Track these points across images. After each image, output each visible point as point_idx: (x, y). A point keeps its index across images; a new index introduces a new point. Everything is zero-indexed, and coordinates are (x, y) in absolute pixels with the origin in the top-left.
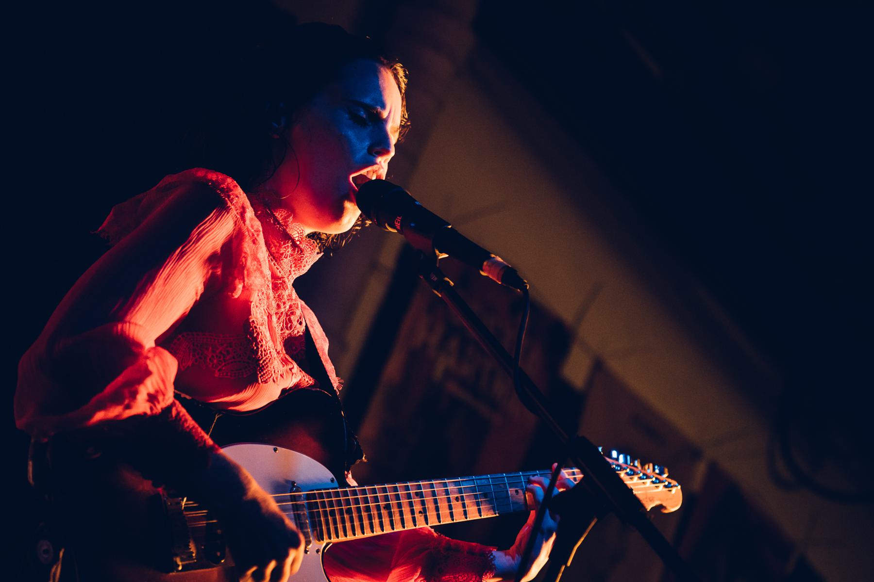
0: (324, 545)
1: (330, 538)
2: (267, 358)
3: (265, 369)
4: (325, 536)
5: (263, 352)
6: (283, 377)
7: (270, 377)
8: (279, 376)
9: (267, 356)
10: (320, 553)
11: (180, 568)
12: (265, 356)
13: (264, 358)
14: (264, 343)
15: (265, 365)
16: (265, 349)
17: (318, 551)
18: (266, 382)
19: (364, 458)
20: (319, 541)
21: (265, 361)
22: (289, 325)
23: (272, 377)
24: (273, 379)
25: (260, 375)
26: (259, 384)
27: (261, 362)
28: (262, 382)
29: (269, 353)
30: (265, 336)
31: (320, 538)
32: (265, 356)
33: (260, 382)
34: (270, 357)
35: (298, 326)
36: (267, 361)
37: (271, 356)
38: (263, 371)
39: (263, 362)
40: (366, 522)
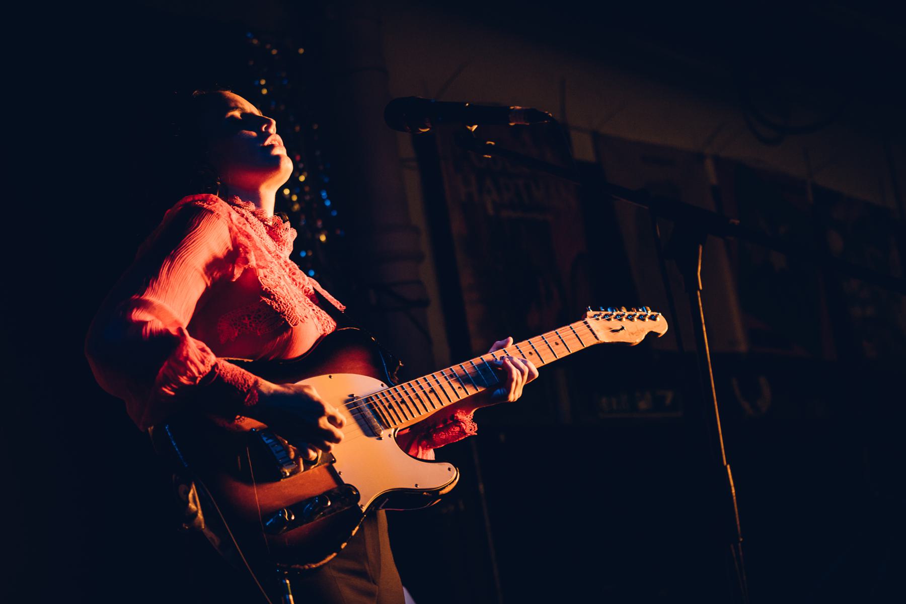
0: (393, 430)
1: (395, 424)
2: (289, 309)
4: (392, 424)
5: (284, 306)
9: (288, 307)
10: (392, 436)
11: (288, 474)
12: (287, 307)
13: (287, 309)
17: (390, 436)
18: (295, 325)
19: (401, 364)
20: (388, 428)
21: (288, 311)
24: (301, 321)
25: (289, 321)
26: (292, 327)
27: (286, 312)
28: (293, 325)
29: (289, 304)
31: (387, 427)
32: (287, 307)
33: (292, 326)
34: (291, 307)
36: (290, 310)
38: (290, 318)
40: (420, 407)
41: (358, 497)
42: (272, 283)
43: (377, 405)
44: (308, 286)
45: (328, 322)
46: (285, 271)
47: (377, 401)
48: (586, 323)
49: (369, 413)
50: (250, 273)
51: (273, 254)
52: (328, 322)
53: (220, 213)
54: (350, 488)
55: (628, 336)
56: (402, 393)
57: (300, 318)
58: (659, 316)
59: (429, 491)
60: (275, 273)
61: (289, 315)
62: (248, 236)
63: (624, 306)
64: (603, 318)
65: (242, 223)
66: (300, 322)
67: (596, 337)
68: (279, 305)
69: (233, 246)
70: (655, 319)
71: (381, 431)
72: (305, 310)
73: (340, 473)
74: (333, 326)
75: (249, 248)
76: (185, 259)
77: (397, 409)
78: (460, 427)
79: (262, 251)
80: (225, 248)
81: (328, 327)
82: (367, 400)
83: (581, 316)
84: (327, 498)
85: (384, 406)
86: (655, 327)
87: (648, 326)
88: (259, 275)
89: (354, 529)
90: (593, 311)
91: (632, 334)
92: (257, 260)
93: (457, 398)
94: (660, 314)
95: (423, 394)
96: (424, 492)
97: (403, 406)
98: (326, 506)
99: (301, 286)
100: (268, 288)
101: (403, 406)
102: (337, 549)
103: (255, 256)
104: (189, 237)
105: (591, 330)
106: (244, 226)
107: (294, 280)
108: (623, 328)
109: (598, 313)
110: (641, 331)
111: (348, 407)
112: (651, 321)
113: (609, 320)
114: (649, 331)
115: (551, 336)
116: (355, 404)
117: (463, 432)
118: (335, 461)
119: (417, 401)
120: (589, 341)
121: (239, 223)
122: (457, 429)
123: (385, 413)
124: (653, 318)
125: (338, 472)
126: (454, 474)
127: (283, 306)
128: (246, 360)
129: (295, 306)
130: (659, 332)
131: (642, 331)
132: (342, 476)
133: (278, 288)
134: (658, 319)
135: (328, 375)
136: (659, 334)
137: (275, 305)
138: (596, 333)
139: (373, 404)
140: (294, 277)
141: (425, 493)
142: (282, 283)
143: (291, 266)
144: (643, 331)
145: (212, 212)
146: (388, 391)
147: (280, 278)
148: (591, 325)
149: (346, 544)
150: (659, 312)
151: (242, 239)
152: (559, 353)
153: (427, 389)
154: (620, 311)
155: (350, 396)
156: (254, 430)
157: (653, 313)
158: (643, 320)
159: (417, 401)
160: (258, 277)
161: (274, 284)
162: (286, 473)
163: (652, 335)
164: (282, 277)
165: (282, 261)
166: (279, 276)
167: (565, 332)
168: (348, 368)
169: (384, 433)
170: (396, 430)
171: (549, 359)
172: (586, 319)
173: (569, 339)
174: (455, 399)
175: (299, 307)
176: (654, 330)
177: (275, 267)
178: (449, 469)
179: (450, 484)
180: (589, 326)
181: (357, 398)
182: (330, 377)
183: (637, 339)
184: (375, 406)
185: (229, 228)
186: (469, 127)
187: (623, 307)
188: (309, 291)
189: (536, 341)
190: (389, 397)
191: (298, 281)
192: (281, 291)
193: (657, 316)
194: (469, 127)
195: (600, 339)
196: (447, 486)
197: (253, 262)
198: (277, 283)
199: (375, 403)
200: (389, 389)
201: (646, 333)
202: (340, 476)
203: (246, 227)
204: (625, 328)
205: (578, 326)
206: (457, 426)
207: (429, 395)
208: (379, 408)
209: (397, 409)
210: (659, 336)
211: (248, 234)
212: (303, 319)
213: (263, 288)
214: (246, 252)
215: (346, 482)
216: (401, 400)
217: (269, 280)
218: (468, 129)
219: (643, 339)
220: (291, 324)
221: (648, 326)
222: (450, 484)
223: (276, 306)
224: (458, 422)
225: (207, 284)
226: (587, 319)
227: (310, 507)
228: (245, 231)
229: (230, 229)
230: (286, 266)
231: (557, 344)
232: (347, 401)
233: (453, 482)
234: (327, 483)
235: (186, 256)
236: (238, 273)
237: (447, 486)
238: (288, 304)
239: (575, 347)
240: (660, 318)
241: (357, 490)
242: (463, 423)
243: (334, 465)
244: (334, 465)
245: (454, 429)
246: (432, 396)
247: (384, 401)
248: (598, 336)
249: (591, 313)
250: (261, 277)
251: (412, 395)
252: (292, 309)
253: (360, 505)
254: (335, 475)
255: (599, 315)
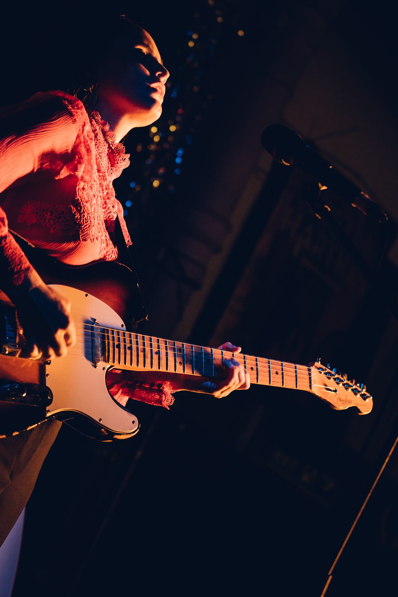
0: (109, 366)
1: (114, 362)
2: (87, 225)
3: (85, 232)
5: (85, 220)
6: (97, 239)
7: (89, 238)
8: (95, 238)
9: (88, 223)
10: (105, 370)
11: (7, 352)
12: (86, 223)
13: (85, 224)
14: (86, 214)
15: (86, 229)
16: (87, 218)
17: (104, 369)
18: (85, 240)
19: (147, 318)
20: (106, 362)
21: (84, 227)
22: (104, 206)
23: (90, 238)
24: (91, 239)
25: (81, 235)
26: (81, 241)
27: (83, 226)
28: (82, 240)
29: (89, 221)
30: (88, 209)
31: (106, 360)
32: (86, 223)
33: (81, 240)
34: (90, 224)
35: (111, 208)
36: (87, 226)
37: (91, 223)
38: (83, 233)
39: (84, 227)
40: (141, 359)
41: (50, 402)
42: (86, 197)
43: (108, 339)
44: (113, 214)
45: (113, 251)
46: (103, 193)
47: (110, 335)
48: (309, 370)
49: (98, 341)
50: (73, 180)
51: (101, 174)
52: (113, 251)
53: (78, 120)
54: (48, 392)
55: (336, 400)
56: (134, 340)
57: (91, 237)
58: (369, 398)
59: (107, 430)
60: (93, 191)
61: (84, 230)
62: (88, 150)
63: (347, 375)
64: (326, 374)
65: (90, 137)
66: (89, 240)
67: (310, 386)
68: (81, 217)
69: (72, 151)
70: (365, 399)
71: (99, 361)
72: (99, 232)
73: (48, 375)
74: (114, 257)
75: (84, 160)
76: (29, 141)
77: (122, 351)
78: (161, 397)
79: (92, 168)
80: (65, 149)
81: (110, 256)
82: (103, 331)
83: (309, 363)
84: (26, 389)
85: (114, 344)
86: (361, 405)
87: (356, 401)
88: (78, 185)
89: (31, 426)
90: (321, 364)
91: (340, 400)
92: (84, 172)
93: (174, 370)
94: (371, 398)
95: (149, 352)
96: (103, 428)
97: (128, 352)
98: (20, 395)
99: (109, 211)
100: (80, 200)
101: (128, 352)
102: (9, 434)
103: (85, 168)
104: (43, 125)
105: (310, 378)
106: (90, 140)
107: (105, 203)
108: (335, 391)
109: (324, 367)
110: (348, 401)
111: (86, 328)
112: (361, 399)
113: (329, 378)
114: (354, 405)
115: (276, 364)
116: (92, 328)
117: (160, 401)
118: (49, 364)
119: (141, 354)
120: (303, 386)
121: (88, 136)
122: (157, 397)
123: (111, 349)
124: (364, 397)
125: (47, 373)
126: (135, 428)
127: (83, 220)
128: (29, 244)
129: (93, 226)
130: (361, 410)
131: (349, 403)
132: (47, 378)
133: (88, 203)
134: (367, 400)
135: (86, 293)
136: (361, 412)
137: (78, 216)
138: (313, 382)
139: (106, 336)
140: (107, 201)
141: (103, 430)
142: (94, 202)
143: (110, 191)
144: (350, 402)
145: (71, 115)
146: (124, 333)
147: (94, 196)
148: (312, 375)
149: (17, 433)
150: (371, 396)
151: (83, 150)
152: (274, 382)
153: (155, 350)
154: (342, 376)
155: (92, 319)
156: (2, 302)
157: (366, 393)
158: (356, 394)
159: (141, 354)
160: (77, 186)
161: (87, 198)
162: (6, 351)
163: (354, 410)
164: (96, 197)
165: (105, 183)
166: (95, 194)
167: (289, 367)
168: (104, 296)
169: (101, 364)
170: (111, 367)
171: (263, 381)
172: (312, 367)
173: (288, 375)
174: (171, 370)
175: (96, 227)
176: (359, 407)
177: (96, 186)
178: (133, 422)
179: (127, 434)
180: (310, 374)
181: (97, 324)
182: (86, 295)
183: (341, 407)
184: (106, 339)
185: (78, 135)
186: (320, 185)
187: (346, 375)
188: (113, 218)
189: (262, 362)
190: (121, 338)
191: (109, 205)
192: (89, 208)
193: (368, 397)
194: (320, 185)
195: (312, 390)
196: (124, 434)
197: (79, 174)
198: (90, 199)
199: (108, 336)
200: (126, 332)
201: (351, 406)
202: (46, 377)
203: (91, 142)
204: (337, 392)
205: (302, 369)
206: (159, 395)
207: (153, 355)
208: (109, 343)
209: (122, 351)
210: (360, 414)
211: (90, 148)
212: (93, 239)
213: (77, 197)
214: (80, 162)
215: (47, 385)
216: (129, 346)
217: (85, 193)
218: (318, 186)
219: (346, 408)
220: (81, 238)
221: (356, 401)
222: (127, 434)
223: (78, 217)
224: (161, 392)
225: (34, 169)
226: (313, 369)
227: (8, 388)
228: (89, 146)
229: (78, 136)
230: (106, 189)
231: (277, 373)
232: (87, 322)
233: (130, 433)
234: (33, 377)
235: (31, 139)
236: (64, 173)
237: (124, 434)
238: (89, 220)
239: (289, 384)
240: (370, 401)
241: (52, 396)
242: (165, 395)
243: (47, 366)
244: (47, 366)
245: (155, 395)
246: (155, 357)
247: (116, 339)
248: (312, 386)
249: (318, 364)
250: (79, 188)
251: (140, 347)
252: (89, 227)
253: (47, 409)
254: (42, 374)
255: (323, 370)
